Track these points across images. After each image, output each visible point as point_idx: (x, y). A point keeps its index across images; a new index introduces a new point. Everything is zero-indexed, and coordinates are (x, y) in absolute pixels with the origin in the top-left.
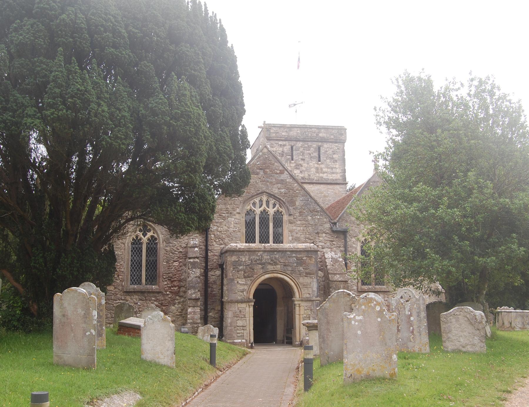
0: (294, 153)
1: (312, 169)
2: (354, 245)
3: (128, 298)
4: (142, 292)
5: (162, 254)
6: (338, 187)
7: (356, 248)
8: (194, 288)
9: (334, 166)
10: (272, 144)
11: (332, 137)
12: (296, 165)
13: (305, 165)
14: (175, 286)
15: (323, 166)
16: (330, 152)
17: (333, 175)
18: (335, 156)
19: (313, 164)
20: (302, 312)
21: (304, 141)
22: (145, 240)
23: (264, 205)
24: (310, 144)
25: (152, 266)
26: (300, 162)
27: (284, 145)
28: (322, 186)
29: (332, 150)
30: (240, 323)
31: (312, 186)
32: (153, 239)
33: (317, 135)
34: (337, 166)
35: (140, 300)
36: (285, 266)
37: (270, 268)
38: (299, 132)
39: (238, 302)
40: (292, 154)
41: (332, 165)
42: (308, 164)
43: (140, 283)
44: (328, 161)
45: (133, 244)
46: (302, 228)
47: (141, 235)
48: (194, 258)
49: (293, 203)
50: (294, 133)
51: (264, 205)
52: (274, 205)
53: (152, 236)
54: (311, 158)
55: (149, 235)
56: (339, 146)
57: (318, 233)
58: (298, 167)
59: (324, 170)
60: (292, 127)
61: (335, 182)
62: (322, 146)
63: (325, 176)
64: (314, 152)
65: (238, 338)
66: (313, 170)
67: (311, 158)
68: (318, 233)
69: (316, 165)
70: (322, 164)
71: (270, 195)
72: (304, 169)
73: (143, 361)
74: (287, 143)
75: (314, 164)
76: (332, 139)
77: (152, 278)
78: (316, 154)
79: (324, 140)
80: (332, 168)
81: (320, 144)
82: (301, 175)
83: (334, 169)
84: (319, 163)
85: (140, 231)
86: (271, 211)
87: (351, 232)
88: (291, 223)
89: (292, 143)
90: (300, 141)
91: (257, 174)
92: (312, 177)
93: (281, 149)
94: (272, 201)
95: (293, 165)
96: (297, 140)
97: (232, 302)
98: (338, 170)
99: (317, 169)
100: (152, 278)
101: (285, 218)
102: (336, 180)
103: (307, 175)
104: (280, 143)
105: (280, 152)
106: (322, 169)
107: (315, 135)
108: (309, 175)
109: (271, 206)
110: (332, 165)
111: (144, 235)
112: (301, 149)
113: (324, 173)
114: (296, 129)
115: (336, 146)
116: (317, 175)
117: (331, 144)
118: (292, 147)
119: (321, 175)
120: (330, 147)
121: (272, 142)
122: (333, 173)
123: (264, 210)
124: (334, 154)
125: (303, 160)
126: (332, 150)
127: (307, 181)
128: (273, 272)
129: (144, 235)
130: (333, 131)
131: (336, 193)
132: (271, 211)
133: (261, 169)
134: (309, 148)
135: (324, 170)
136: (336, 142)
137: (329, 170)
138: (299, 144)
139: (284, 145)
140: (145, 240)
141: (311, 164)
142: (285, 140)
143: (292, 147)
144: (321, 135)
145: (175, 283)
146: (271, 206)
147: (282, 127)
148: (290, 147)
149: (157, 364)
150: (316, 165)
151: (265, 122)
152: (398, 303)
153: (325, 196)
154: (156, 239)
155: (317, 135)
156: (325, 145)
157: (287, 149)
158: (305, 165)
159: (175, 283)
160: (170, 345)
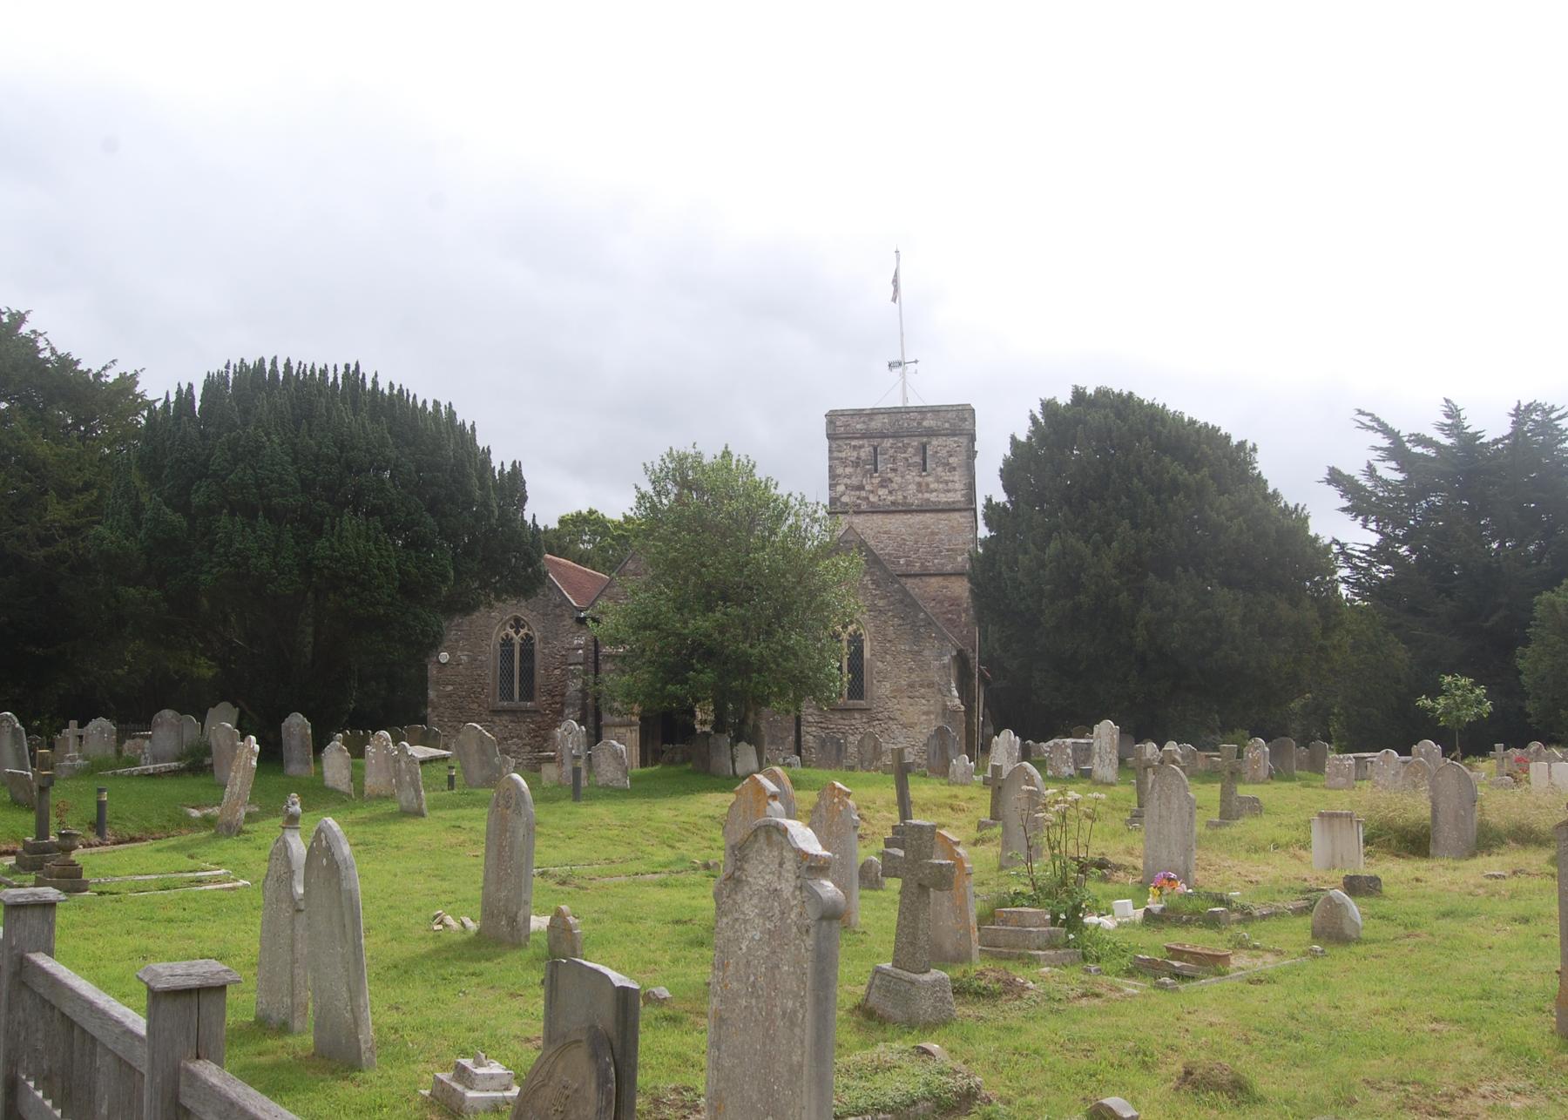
3: (496, 719)
4: (512, 712)
5: (538, 657)
6: (957, 515)
8: (573, 705)
13: (898, 479)
15: (930, 479)
16: (943, 453)
18: (951, 460)
19: (913, 476)
22: (517, 639)
25: (528, 674)
32: (528, 639)
41: (947, 476)
47: (512, 632)
50: (876, 424)
55: (523, 631)
60: (874, 413)
63: (933, 497)
66: (913, 487)
69: (918, 479)
73: (326, 788)
74: (865, 442)
77: (528, 694)
78: (918, 459)
79: (932, 433)
80: (947, 482)
92: (909, 500)
95: (876, 481)
96: (884, 436)
97: (607, 725)
98: (958, 486)
99: (919, 484)
100: (528, 694)
110: (947, 476)
111: (517, 633)
112: (891, 452)
118: (875, 449)
119: (927, 495)
129: (517, 633)
134: (905, 447)
138: (888, 443)
140: (517, 639)
143: (875, 449)
144: (925, 423)
145: (558, 699)
147: (858, 413)
149: (338, 791)
150: (918, 479)
153: (933, 533)
156: (935, 442)
157: (865, 453)
158: (898, 479)
159: (558, 699)
160: (346, 773)
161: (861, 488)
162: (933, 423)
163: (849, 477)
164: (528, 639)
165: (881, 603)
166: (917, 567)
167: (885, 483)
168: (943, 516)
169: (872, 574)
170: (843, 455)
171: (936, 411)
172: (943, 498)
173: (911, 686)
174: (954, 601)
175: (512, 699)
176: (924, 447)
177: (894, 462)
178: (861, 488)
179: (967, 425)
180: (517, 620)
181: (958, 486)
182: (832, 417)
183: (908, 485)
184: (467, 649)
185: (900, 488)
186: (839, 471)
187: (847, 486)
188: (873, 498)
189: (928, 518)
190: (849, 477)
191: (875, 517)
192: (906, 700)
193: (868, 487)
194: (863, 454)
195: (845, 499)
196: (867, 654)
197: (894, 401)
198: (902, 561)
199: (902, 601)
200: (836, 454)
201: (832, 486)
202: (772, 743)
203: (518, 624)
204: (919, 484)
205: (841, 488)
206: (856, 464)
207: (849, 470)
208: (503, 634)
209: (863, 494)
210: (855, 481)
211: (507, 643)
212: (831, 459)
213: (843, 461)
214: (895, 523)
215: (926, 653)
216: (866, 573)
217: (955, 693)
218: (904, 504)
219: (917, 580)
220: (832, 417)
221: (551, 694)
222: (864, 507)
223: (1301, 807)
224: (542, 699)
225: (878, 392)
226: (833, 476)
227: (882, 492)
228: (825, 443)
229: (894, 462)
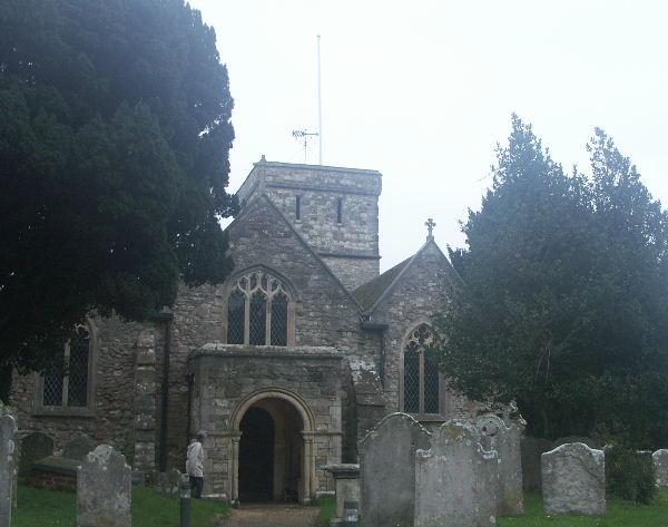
6: (366, 262)
11: (359, 186)
15: (342, 229)
18: (364, 215)
19: (330, 226)
20: (315, 453)
21: (317, 190)
23: (259, 286)
27: (287, 195)
34: (366, 231)
35: (59, 429)
36: (289, 380)
37: (268, 382)
40: (298, 208)
41: (357, 227)
43: (58, 401)
46: (315, 323)
48: (147, 365)
49: (303, 283)
51: (259, 286)
52: (274, 286)
57: (340, 331)
63: (346, 245)
65: (215, 491)
68: (340, 331)
69: (334, 228)
71: (268, 270)
72: (316, 233)
74: (291, 192)
77: (79, 395)
78: (334, 211)
79: (347, 191)
86: (270, 294)
88: (299, 314)
89: (299, 193)
90: (310, 190)
91: (249, 236)
93: (281, 201)
94: (271, 280)
96: (307, 189)
99: (335, 233)
101: (291, 306)
102: (364, 251)
106: (342, 234)
108: (323, 243)
109: (269, 286)
123: (280, 294)
125: (315, 219)
128: (269, 389)
132: (270, 294)
133: (254, 229)
134: (324, 201)
135: (346, 236)
136: (366, 195)
138: (311, 194)
139: (287, 195)
142: (289, 188)
144: (342, 182)
146: (269, 286)
150: (334, 228)
154: (86, 333)
157: (290, 201)
158: (317, 227)
162: (348, 183)
171: (352, 172)
172: (355, 247)
176: (339, 203)
204: (335, 233)
223: (565, 506)
224: (94, 405)
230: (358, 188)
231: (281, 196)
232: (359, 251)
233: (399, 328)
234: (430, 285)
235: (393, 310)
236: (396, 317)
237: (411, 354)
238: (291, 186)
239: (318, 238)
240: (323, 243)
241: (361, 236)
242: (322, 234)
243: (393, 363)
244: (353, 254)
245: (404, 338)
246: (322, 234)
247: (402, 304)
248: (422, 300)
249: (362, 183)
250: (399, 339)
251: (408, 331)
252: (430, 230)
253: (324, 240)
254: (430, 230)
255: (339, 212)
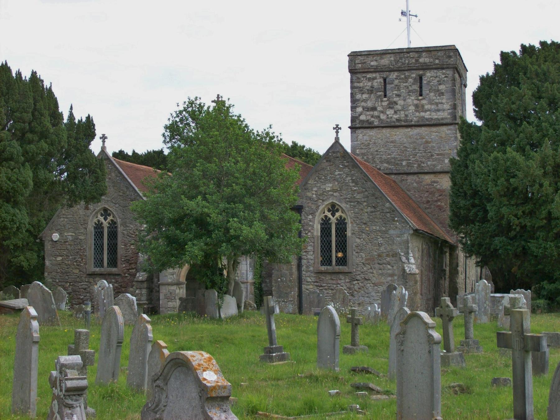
0: (388, 87)
1: (410, 108)
2: (311, 223)
6: (444, 128)
7: (313, 226)
9: (440, 101)
10: (358, 78)
11: (437, 61)
12: (388, 104)
13: (401, 102)
14: (133, 269)
15: (424, 102)
16: (435, 82)
17: (439, 113)
18: (442, 87)
19: (412, 100)
21: (398, 70)
24: (407, 73)
25: (113, 249)
26: (395, 99)
28: (423, 128)
29: (438, 79)
30: (171, 304)
31: (409, 129)
32: (113, 224)
33: (417, 61)
34: (444, 101)
38: (392, 59)
39: (169, 284)
42: (405, 100)
44: (432, 94)
45: (95, 228)
47: (102, 219)
50: (385, 61)
53: (112, 220)
54: (410, 92)
55: (110, 218)
56: (448, 72)
58: (391, 106)
59: (426, 107)
61: (441, 122)
62: (424, 74)
63: (427, 115)
64: (413, 84)
66: (412, 108)
67: (410, 92)
70: (424, 99)
72: (399, 107)
74: (377, 75)
75: (413, 100)
76: (437, 64)
77: (113, 262)
78: (416, 87)
79: (426, 67)
80: (437, 104)
81: (421, 72)
82: (396, 117)
83: (439, 105)
84: (420, 98)
85: (102, 215)
87: (307, 209)
89: (385, 75)
99: (416, 106)
100: (113, 262)
102: (442, 119)
103: (403, 115)
104: (369, 76)
105: (368, 88)
106: (423, 106)
107: (414, 61)
108: (406, 116)
113: (426, 111)
114: (388, 56)
115: (443, 74)
116: (417, 114)
117: (435, 71)
119: (422, 114)
120: (435, 75)
121: (359, 76)
122: (438, 110)
124: (440, 84)
126: (438, 79)
127: (403, 123)
129: (105, 219)
130: (439, 54)
131: (441, 137)
134: (406, 78)
135: (426, 107)
136: (443, 69)
137: (433, 107)
138: (394, 75)
139: (374, 78)
140: (105, 224)
141: (409, 100)
142: (375, 72)
143: (385, 80)
144: (421, 60)
148: (382, 80)
150: (416, 102)
151: (218, 95)
152: (98, 290)
153: (427, 142)
155: (417, 61)
156: (428, 74)
157: (378, 82)
158: (401, 102)
161: (374, 109)
162: (427, 60)
163: (365, 101)
164: (113, 224)
165: (358, 196)
166: (415, 169)
167: (392, 104)
168: (434, 129)
169: (352, 175)
170: (361, 85)
171: (428, 50)
172: (435, 116)
173: (379, 256)
174: (441, 192)
175: (103, 266)
177: (399, 90)
178: (374, 109)
179: (452, 61)
180: (105, 210)
181: (446, 106)
182: (354, 56)
183: (407, 105)
184: (69, 230)
185: (403, 109)
186: (358, 96)
187: (364, 108)
188: (383, 117)
189: (423, 131)
190: (365, 101)
191: (384, 130)
192: (377, 266)
193: (379, 108)
194: (375, 84)
195: (363, 117)
196: (349, 233)
197: (401, 44)
198: (404, 163)
199: (373, 195)
200: (356, 84)
201: (353, 108)
202: (279, 297)
203: (106, 213)
205: (359, 110)
206: (371, 91)
207: (365, 96)
208: (95, 220)
209: (376, 113)
210: (369, 104)
211: (99, 227)
212: (352, 88)
213: (362, 90)
214: (399, 135)
215: (391, 232)
216: (347, 175)
217: (412, 260)
218: (406, 121)
219: (415, 177)
220: (354, 56)
221: (127, 261)
222: (376, 123)
224: (122, 266)
225: (388, 36)
226: (354, 101)
227: (390, 112)
228: (348, 75)
229: (399, 90)
230: (435, 64)
231: (369, 79)
232: (438, 119)
233: (314, 207)
234: (337, 173)
235: (309, 194)
236: (310, 199)
237: (325, 224)
238: (376, 70)
239: (402, 112)
240: (406, 116)
241: (440, 106)
242: (404, 108)
243: (309, 231)
244: (432, 122)
245: (317, 214)
246: (404, 108)
247: (315, 189)
248: (330, 185)
249: (438, 59)
250: (313, 214)
251: (321, 208)
252: (337, 132)
253: (407, 113)
254: (337, 132)
255: (421, 87)
